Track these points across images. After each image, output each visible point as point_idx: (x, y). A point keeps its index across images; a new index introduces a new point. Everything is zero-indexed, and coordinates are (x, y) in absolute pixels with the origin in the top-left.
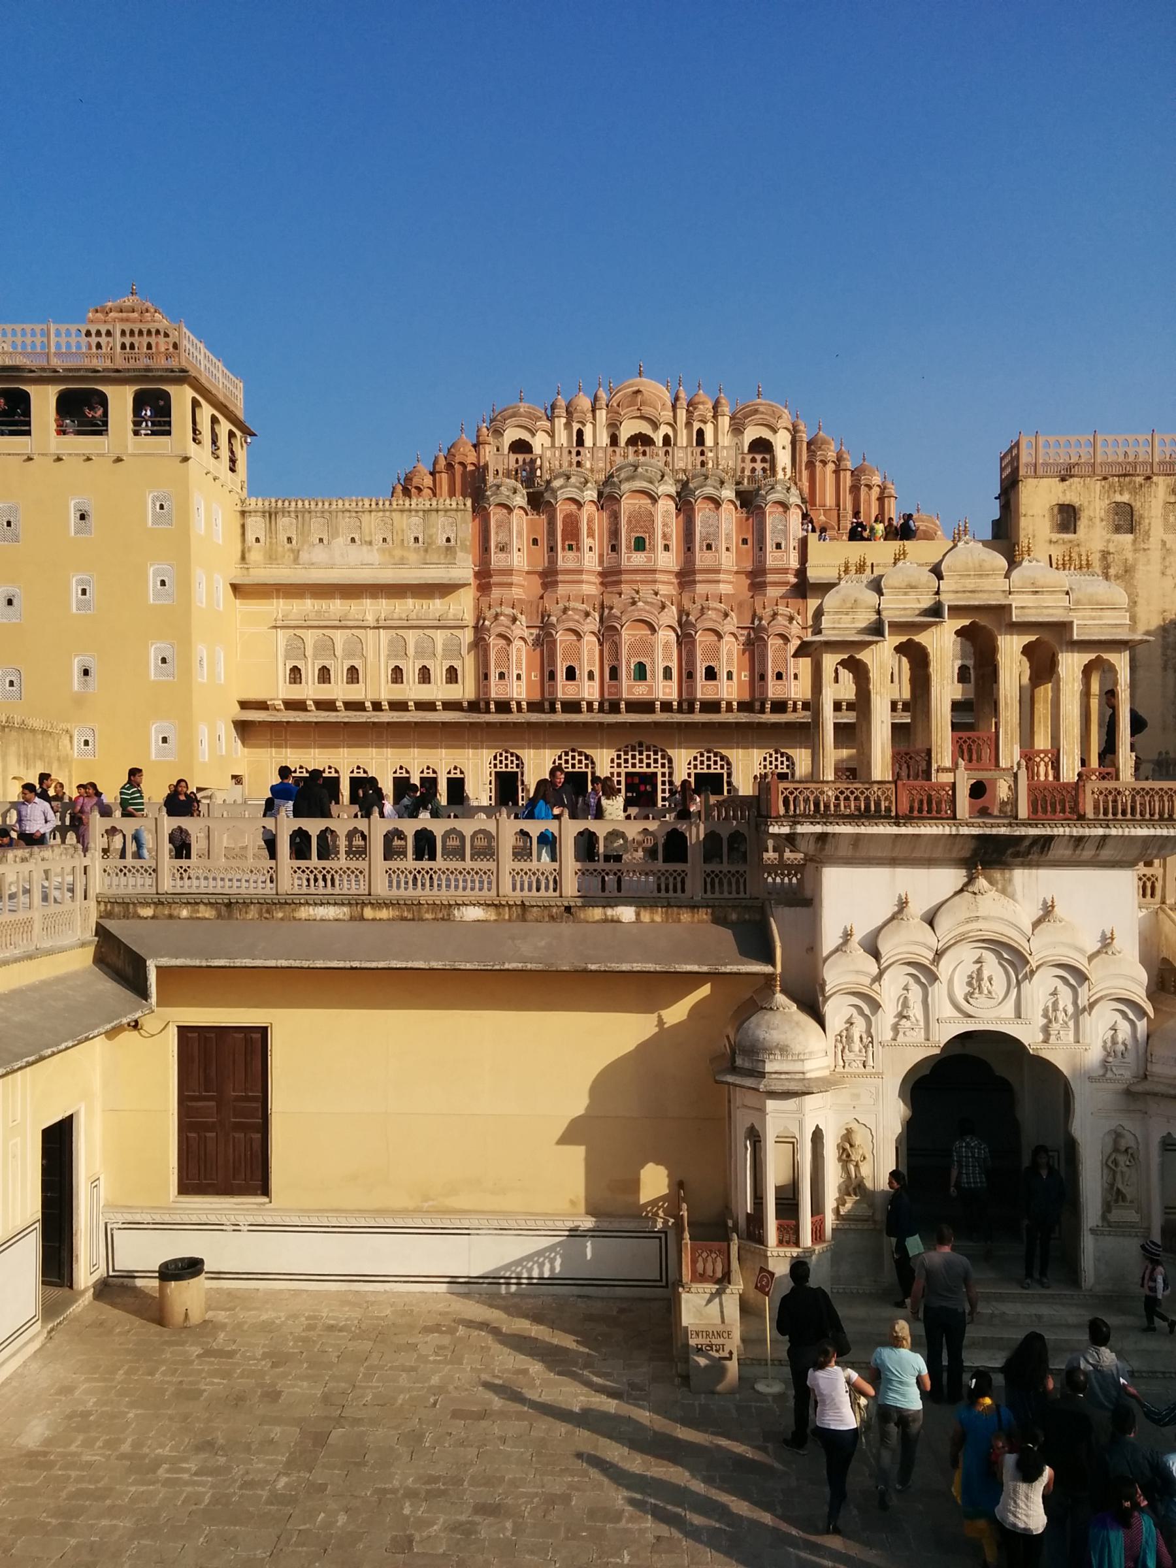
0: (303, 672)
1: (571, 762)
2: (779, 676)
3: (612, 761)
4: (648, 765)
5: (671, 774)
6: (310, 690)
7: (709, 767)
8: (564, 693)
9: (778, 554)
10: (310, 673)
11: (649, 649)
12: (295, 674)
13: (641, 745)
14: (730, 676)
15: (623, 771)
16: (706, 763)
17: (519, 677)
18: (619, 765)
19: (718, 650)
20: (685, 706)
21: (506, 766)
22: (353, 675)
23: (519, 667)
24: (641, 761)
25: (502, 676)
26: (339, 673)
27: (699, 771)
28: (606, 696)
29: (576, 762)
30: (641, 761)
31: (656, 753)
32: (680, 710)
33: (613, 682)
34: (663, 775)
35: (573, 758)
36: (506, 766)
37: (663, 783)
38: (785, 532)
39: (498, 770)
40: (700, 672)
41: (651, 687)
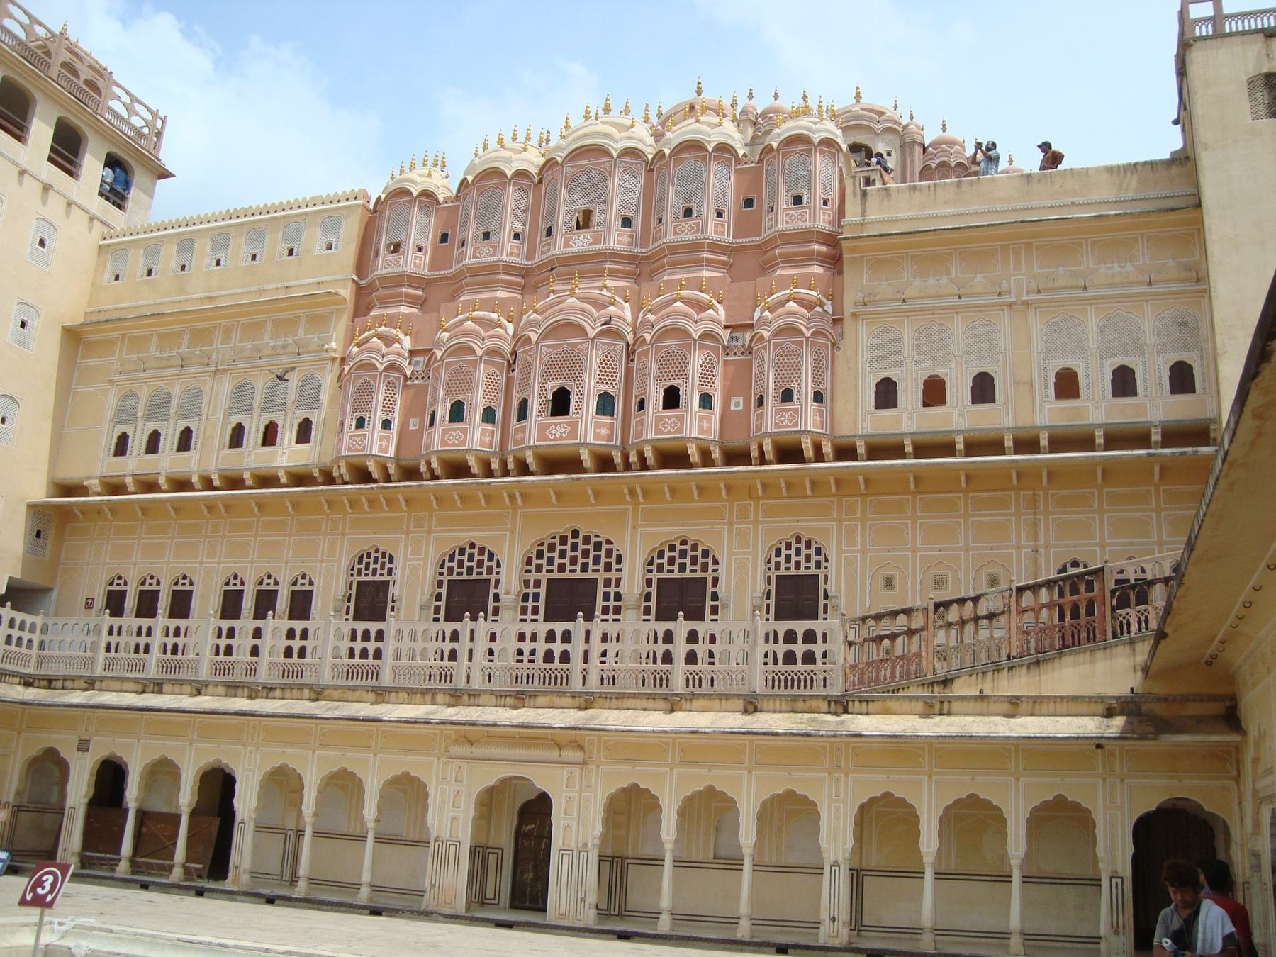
0: (130, 440)
1: (466, 564)
2: (787, 396)
3: (529, 562)
4: (585, 568)
5: (618, 581)
6: (135, 463)
7: (682, 568)
8: (444, 443)
9: (797, 211)
10: (138, 442)
11: (575, 366)
12: (122, 446)
13: (575, 533)
14: (706, 401)
15: (544, 577)
16: (678, 561)
17: (387, 424)
18: (539, 569)
19: (683, 361)
20: (633, 458)
21: (374, 573)
22: (185, 441)
23: (389, 406)
24: (574, 561)
25: (360, 423)
26: (169, 440)
27: (665, 575)
28: (511, 447)
29: (474, 564)
30: (574, 561)
31: (598, 546)
32: (628, 467)
33: (522, 424)
34: (607, 583)
35: (471, 558)
36: (374, 573)
37: (606, 597)
38: (808, 180)
39: (362, 578)
40: (655, 397)
41: (574, 426)
